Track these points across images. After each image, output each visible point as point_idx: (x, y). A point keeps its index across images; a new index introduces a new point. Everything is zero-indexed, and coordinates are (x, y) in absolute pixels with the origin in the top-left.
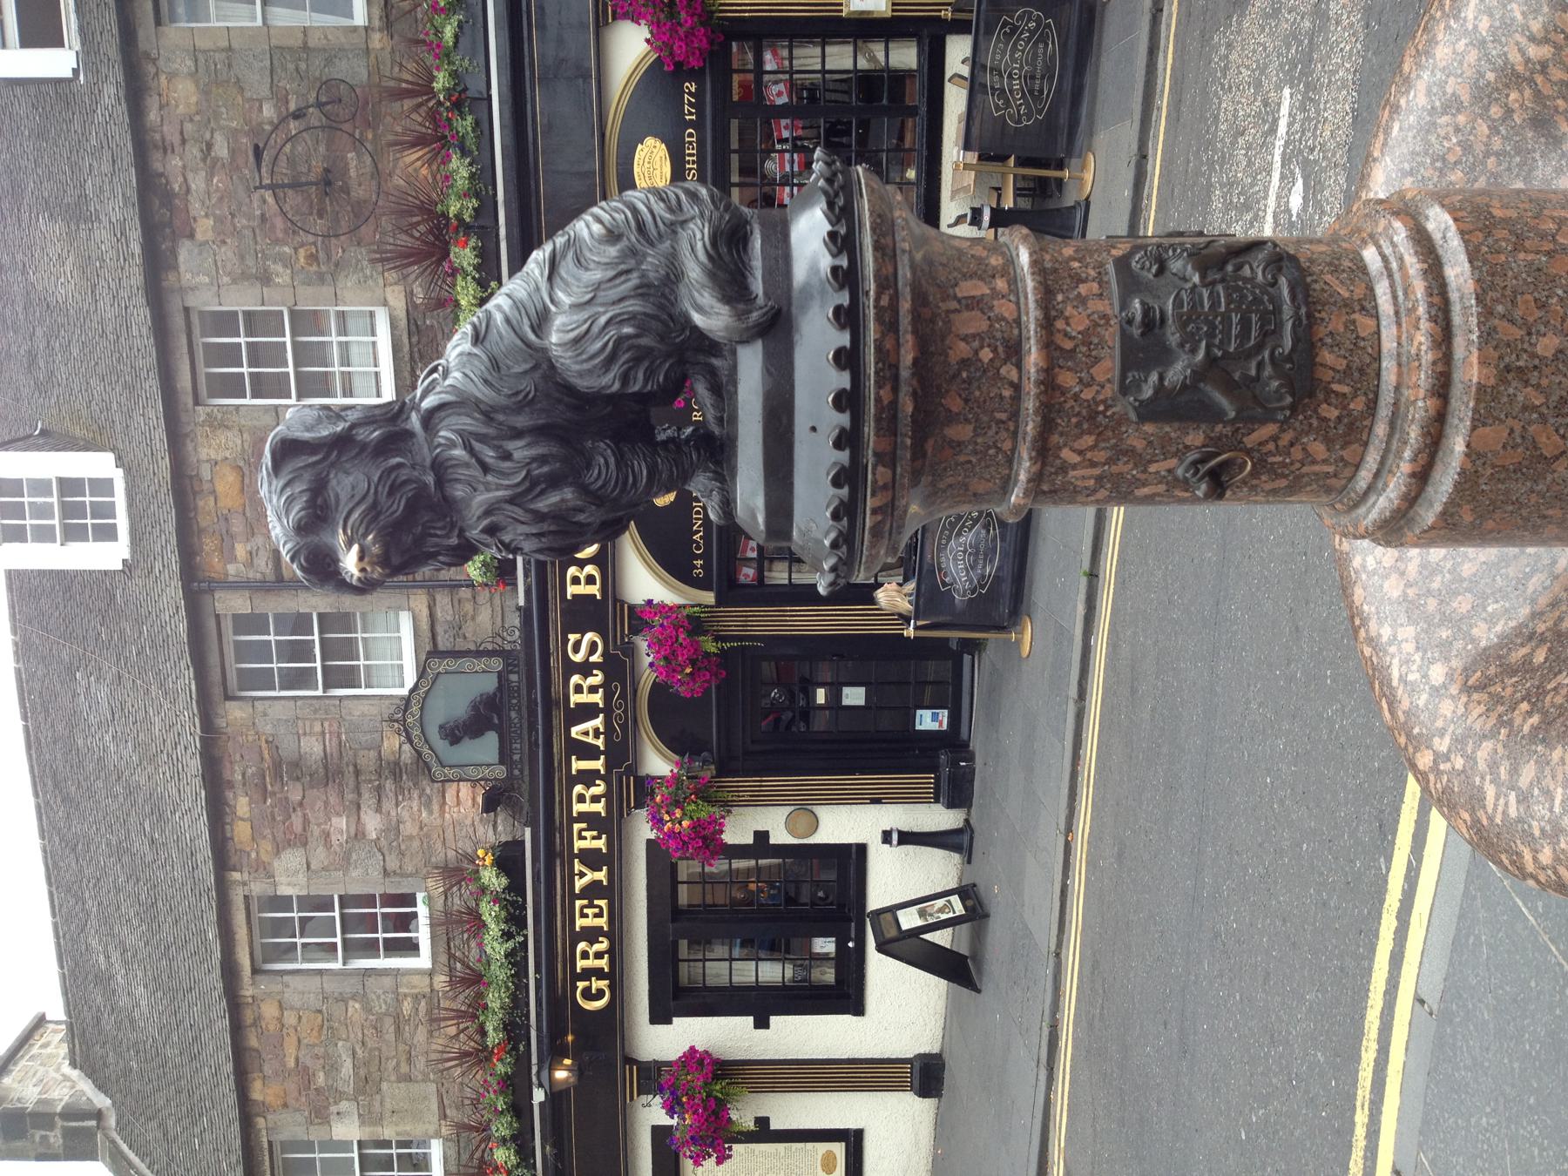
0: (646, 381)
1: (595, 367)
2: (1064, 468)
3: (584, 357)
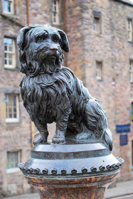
0: (93, 122)
1: (96, 110)
3: (97, 108)
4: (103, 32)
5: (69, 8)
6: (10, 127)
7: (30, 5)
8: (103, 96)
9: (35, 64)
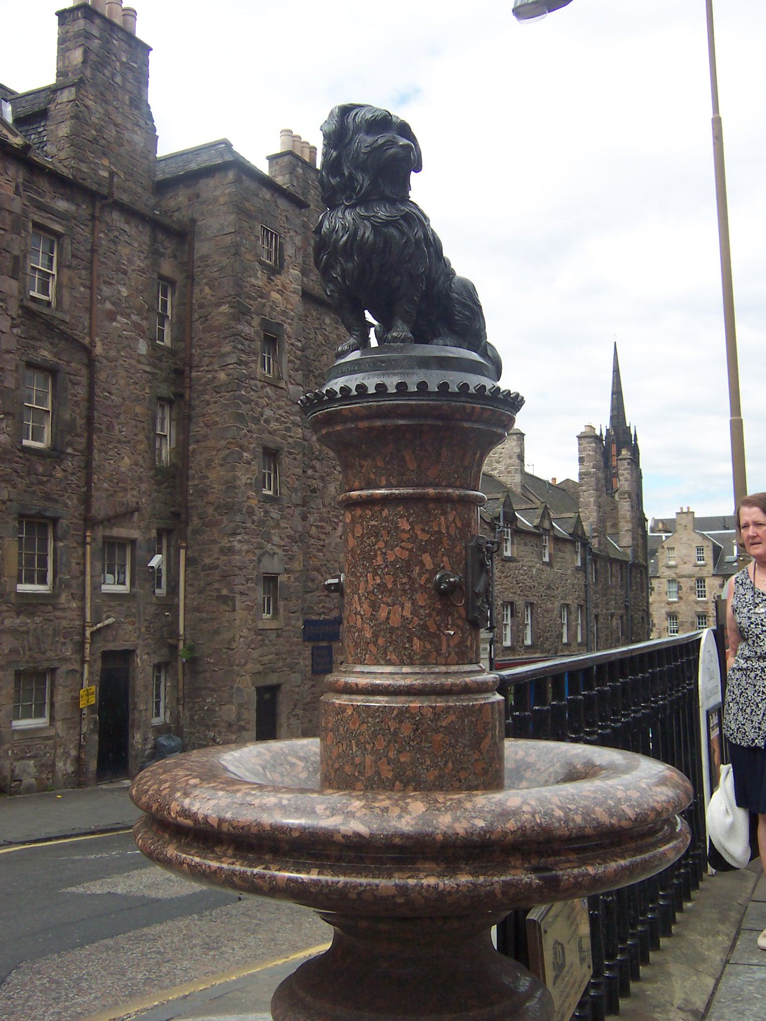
2: (444, 513)
4: (285, 377)
5: (201, 306)
6: (29, 604)
7: (101, 290)
8: (276, 539)
9: (361, 178)
